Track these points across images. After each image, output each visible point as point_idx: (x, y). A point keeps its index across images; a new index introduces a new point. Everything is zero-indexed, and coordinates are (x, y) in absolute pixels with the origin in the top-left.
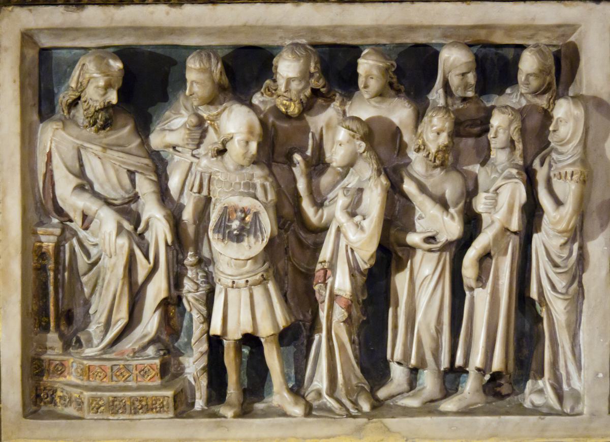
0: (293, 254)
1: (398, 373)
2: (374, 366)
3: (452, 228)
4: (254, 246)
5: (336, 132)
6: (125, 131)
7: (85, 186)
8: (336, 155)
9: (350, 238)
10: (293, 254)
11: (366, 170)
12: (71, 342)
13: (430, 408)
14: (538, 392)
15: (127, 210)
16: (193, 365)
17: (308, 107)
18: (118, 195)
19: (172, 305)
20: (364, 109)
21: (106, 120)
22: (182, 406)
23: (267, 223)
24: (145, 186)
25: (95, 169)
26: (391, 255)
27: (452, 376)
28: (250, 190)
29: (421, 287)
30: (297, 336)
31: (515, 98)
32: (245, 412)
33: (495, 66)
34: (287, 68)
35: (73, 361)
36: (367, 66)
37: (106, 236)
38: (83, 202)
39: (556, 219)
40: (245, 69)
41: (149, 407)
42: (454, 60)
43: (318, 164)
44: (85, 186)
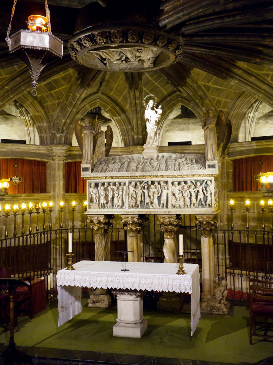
0: (106, 197)
1: (115, 206)
2: (113, 205)
3: (117, 195)
4: (104, 197)
5: (109, 188)
6: (96, 189)
7: (93, 192)
8: (109, 190)
9: (110, 196)
10: (106, 197)
11: (111, 191)
12: (92, 204)
13: (116, 208)
14: (124, 207)
15: (96, 194)
16: (101, 205)
17: (108, 187)
18: (95, 193)
19: (99, 201)
20: (112, 187)
21: (94, 188)
22: (99, 208)
23: (104, 195)
24: (97, 192)
25: (94, 191)
26: (113, 198)
27: (118, 206)
28: (103, 193)
29: (116, 199)
30: (107, 203)
31: (122, 186)
32: (104, 208)
33: (120, 184)
34: (106, 184)
35: (92, 205)
36: (111, 184)
37: (94, 196)
38: (93, 194)
39: (124, 195)
40: (103, 184)
41: (96, 208)
42: (117, 183)
43: (108, 191)
44: (93, 192)
